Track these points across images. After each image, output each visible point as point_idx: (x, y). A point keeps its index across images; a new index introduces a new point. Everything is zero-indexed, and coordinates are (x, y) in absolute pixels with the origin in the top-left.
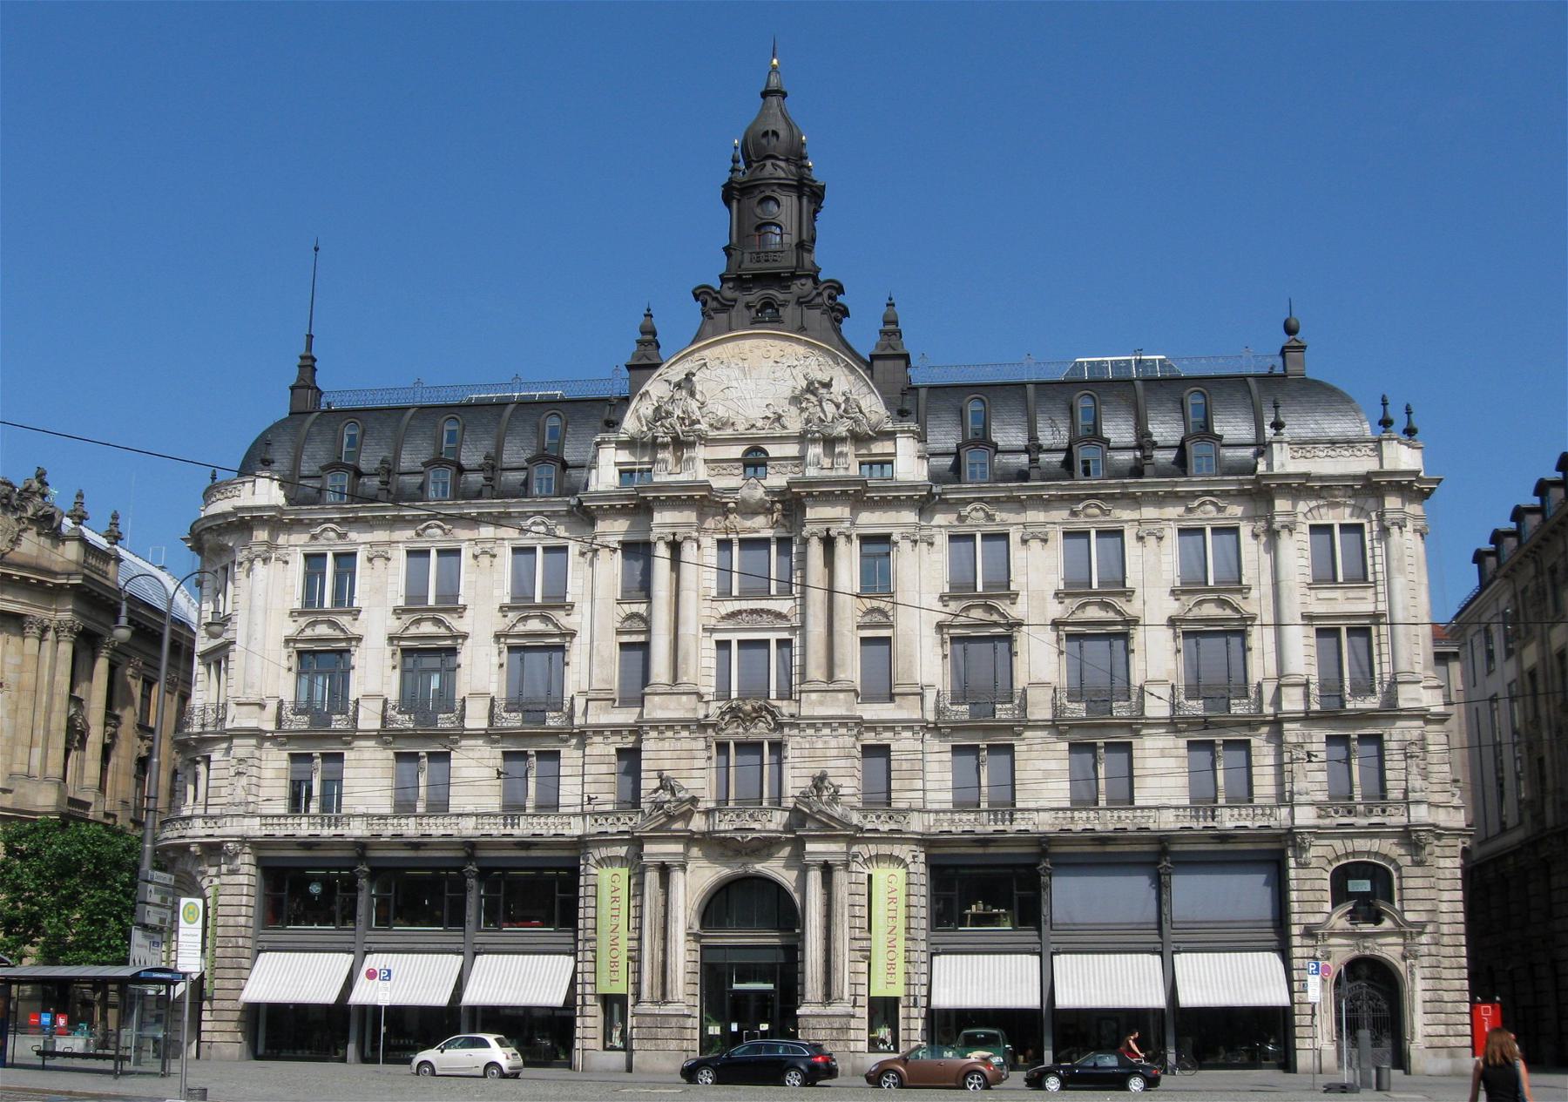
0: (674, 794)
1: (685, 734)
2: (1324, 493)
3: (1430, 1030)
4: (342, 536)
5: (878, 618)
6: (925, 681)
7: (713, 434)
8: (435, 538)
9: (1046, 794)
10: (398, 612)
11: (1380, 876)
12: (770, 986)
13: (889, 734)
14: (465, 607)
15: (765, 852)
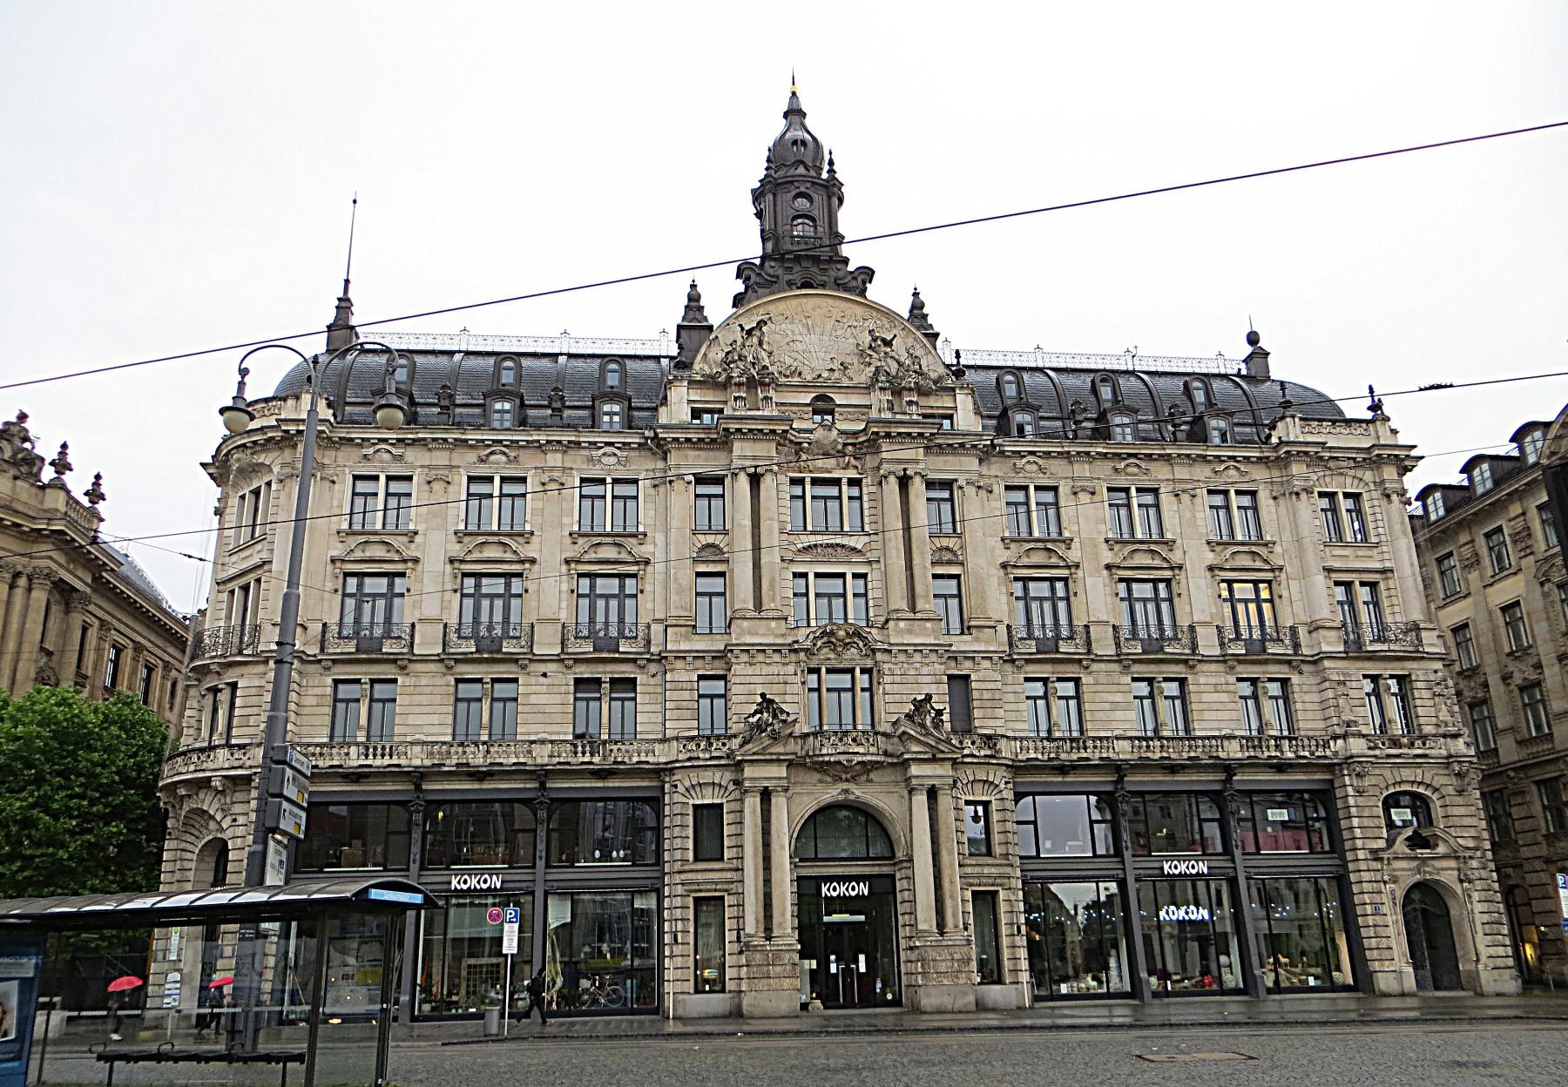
0: (775, 716)
1: (777, 657)
2: (1331, 464)
3: (1492, 951)
4: (399, 458)
5: (947, 556)
6: (996, 617)
7: (783, 380)
9: (1114, 725)
10: (460, 536)
11: (1419, 804)
12: (862, 918)
13: (968, 664)
14: (532, 533)
15: (864, 778)
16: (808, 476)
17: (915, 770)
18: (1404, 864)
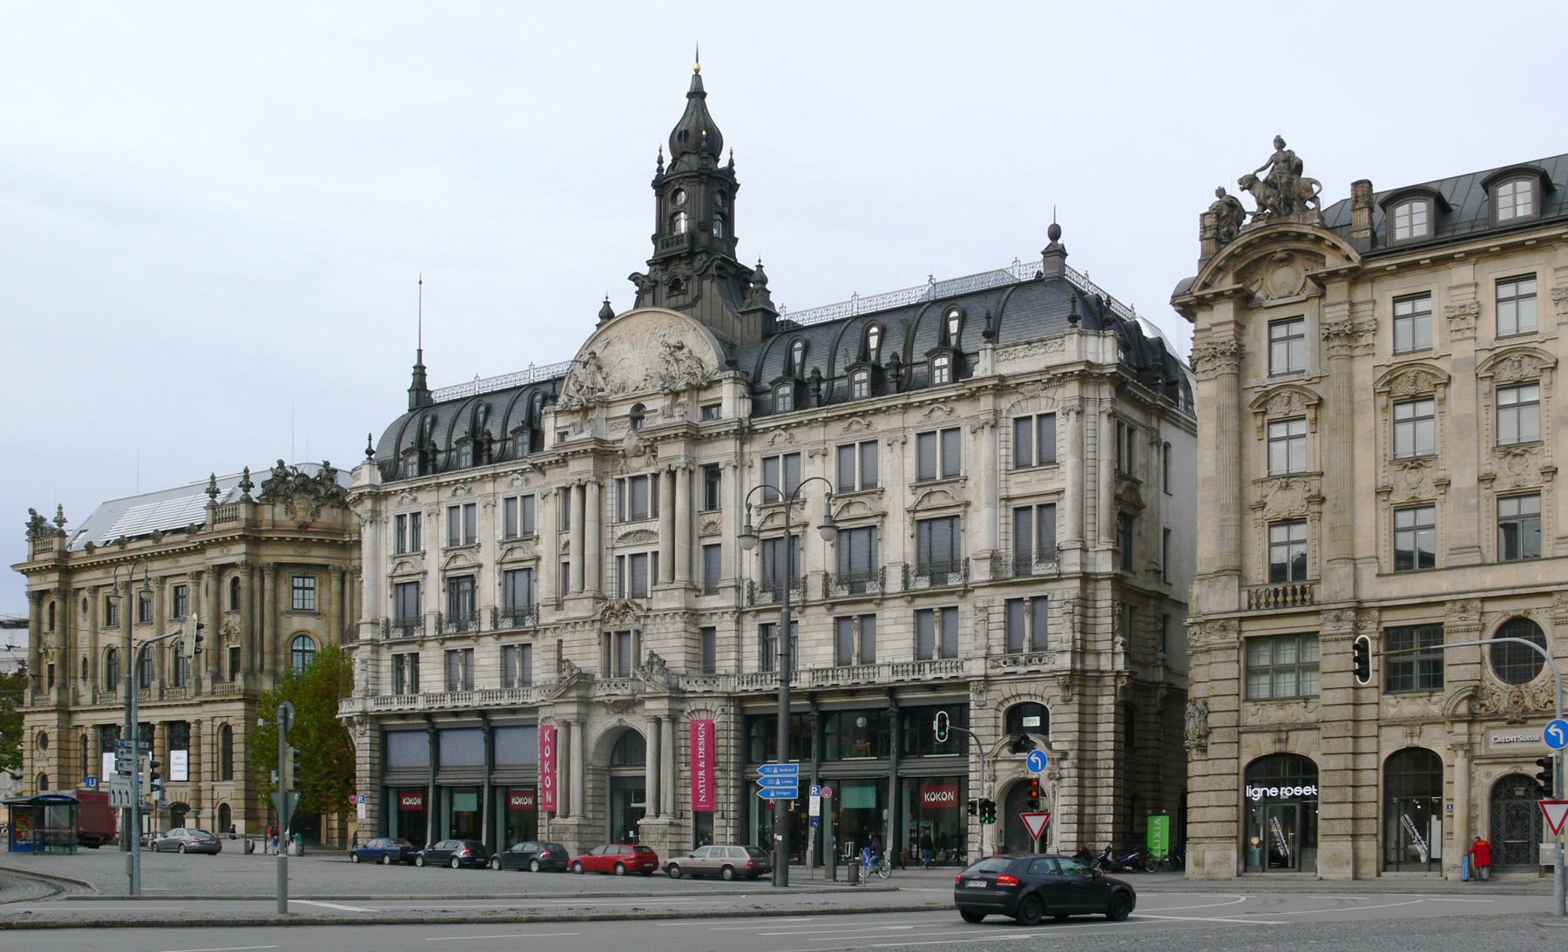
8: (462, 499)
16: (625, 476)
17: (649, 705)
18: (1005, 766)
